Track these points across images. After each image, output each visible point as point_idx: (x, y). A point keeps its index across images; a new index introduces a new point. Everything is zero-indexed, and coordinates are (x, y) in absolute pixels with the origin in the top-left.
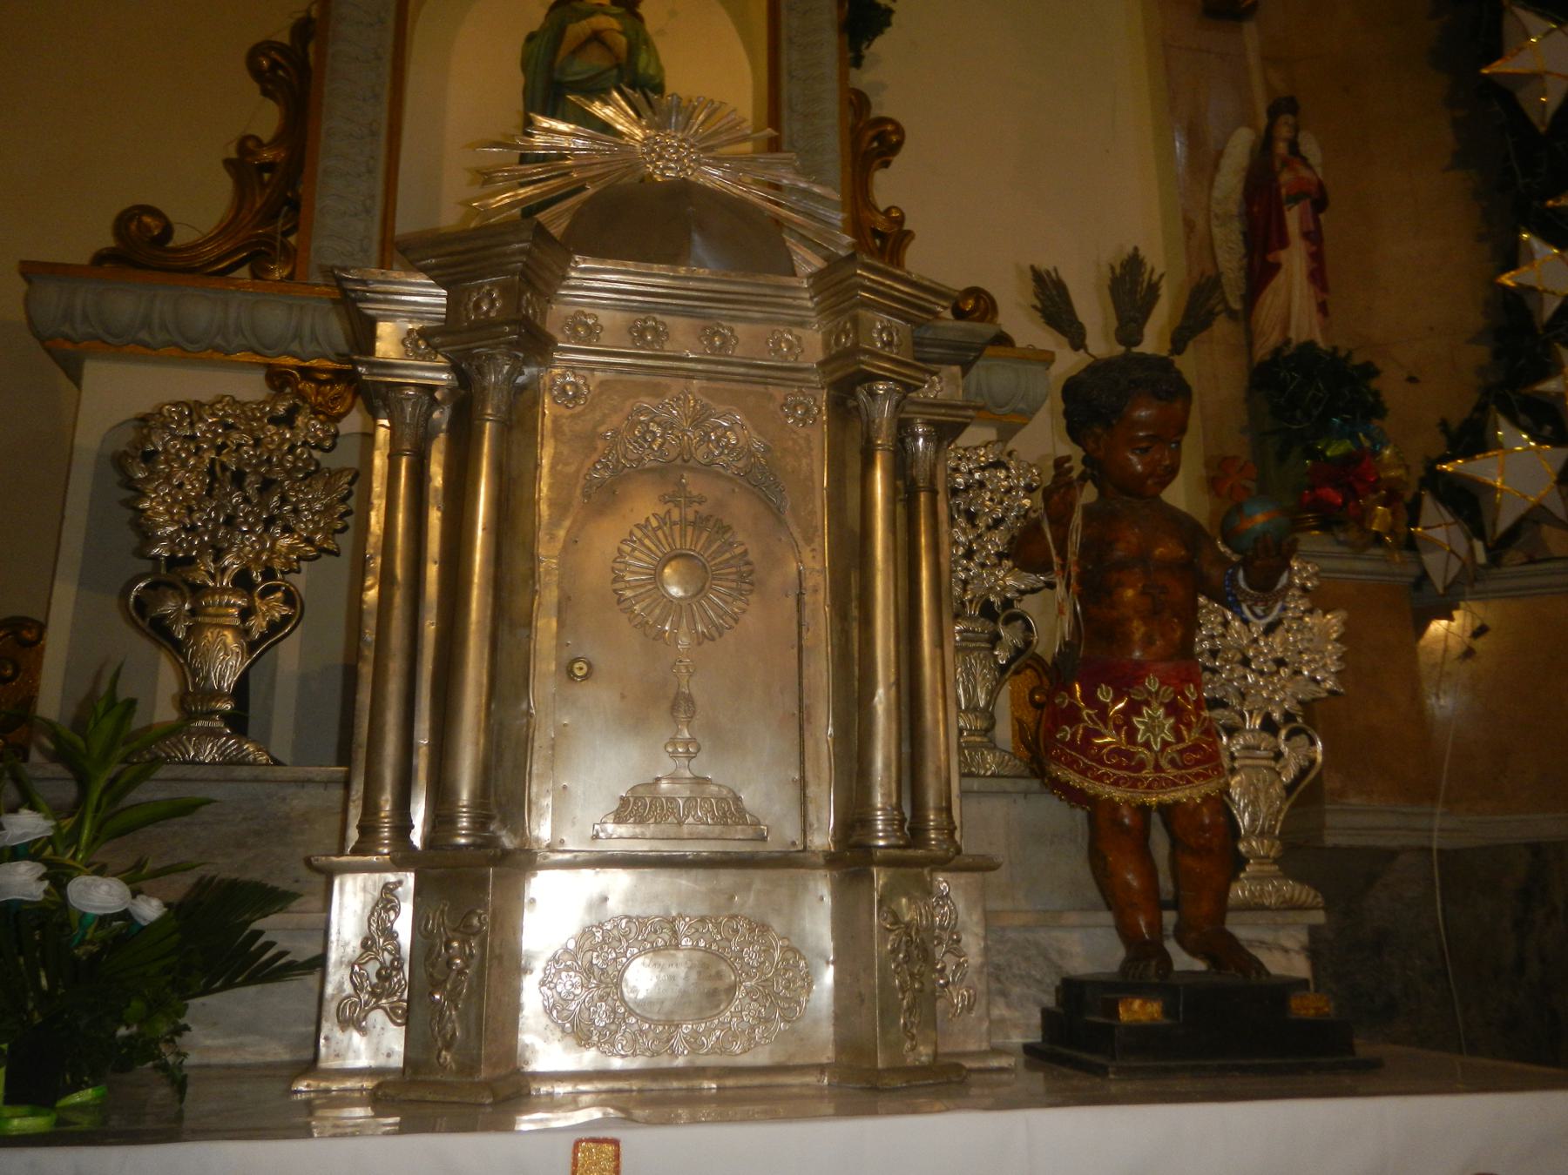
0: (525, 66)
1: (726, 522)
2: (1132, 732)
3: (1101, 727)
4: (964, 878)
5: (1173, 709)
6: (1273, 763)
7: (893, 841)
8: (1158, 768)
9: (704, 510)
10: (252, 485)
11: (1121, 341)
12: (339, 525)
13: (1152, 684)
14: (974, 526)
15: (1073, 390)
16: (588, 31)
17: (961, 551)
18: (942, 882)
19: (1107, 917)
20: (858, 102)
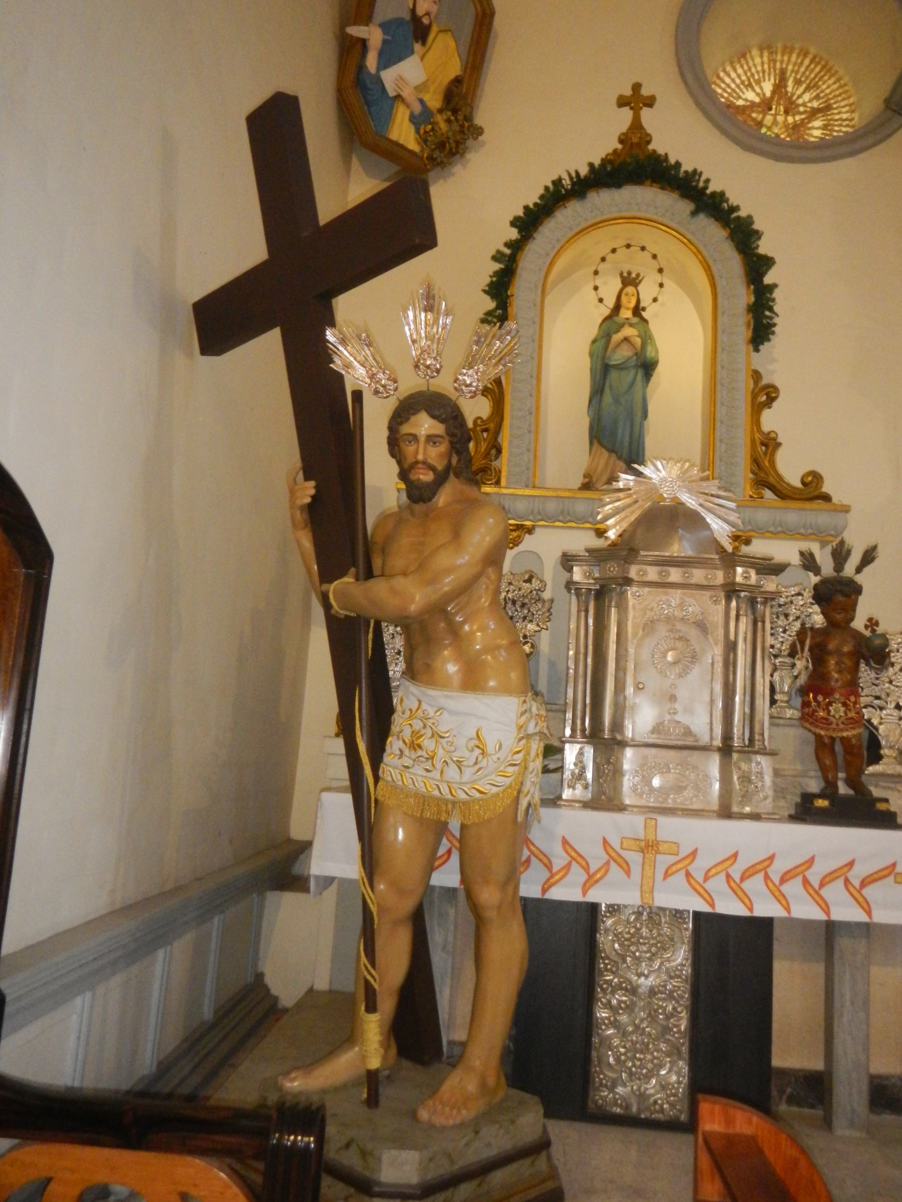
0: (591, 355)
1: (688, 638)
2: (829, 712)
3: (818, 710)
4: (768, 758)
5: (844, 704)
6: (897, 721)
7: (740, 745)
8: (837, 725)
9: (681, 634)
10: (518, 604)
11: (835, 571)
12: (547, 620)
13: (837, 696)
14: (787, 620)
15: (816, 587)
16: (622, 337)
17: (781, 630)
18: (759, 758)
19: (820, 774)
20: (757, 375)
